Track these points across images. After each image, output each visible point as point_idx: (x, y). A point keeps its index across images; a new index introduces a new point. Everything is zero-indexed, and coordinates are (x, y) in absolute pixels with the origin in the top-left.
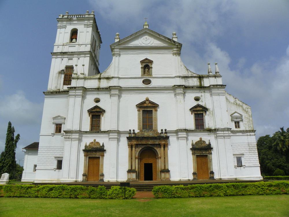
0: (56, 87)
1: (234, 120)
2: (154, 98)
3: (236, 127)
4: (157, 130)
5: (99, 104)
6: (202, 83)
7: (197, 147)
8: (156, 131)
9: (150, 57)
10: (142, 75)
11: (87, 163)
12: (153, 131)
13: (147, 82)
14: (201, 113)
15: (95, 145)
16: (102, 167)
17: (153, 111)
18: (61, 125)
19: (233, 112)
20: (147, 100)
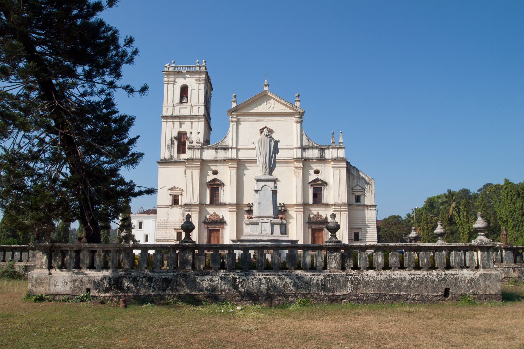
6: (324, 154)
14: (320, 186)
15: (214, 217)
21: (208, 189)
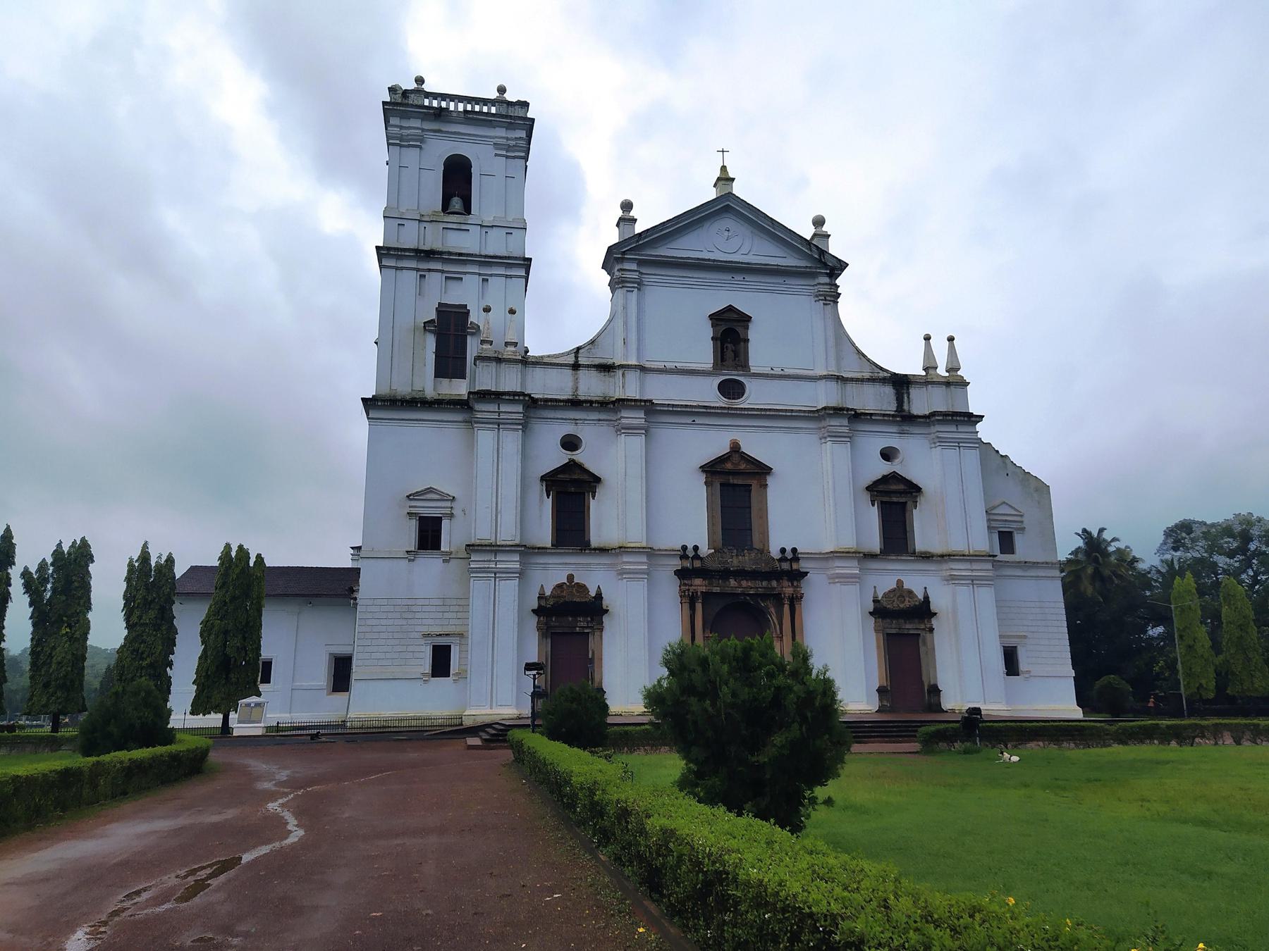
2: (758, 444)
5: (580, 456)
8: (764, 551)
10: (715, 364)
13: (731, 389)
14: (902, 500)
17: (753, 488)
18: (438, 521)
20: (735, 448)
21: (548, 498)
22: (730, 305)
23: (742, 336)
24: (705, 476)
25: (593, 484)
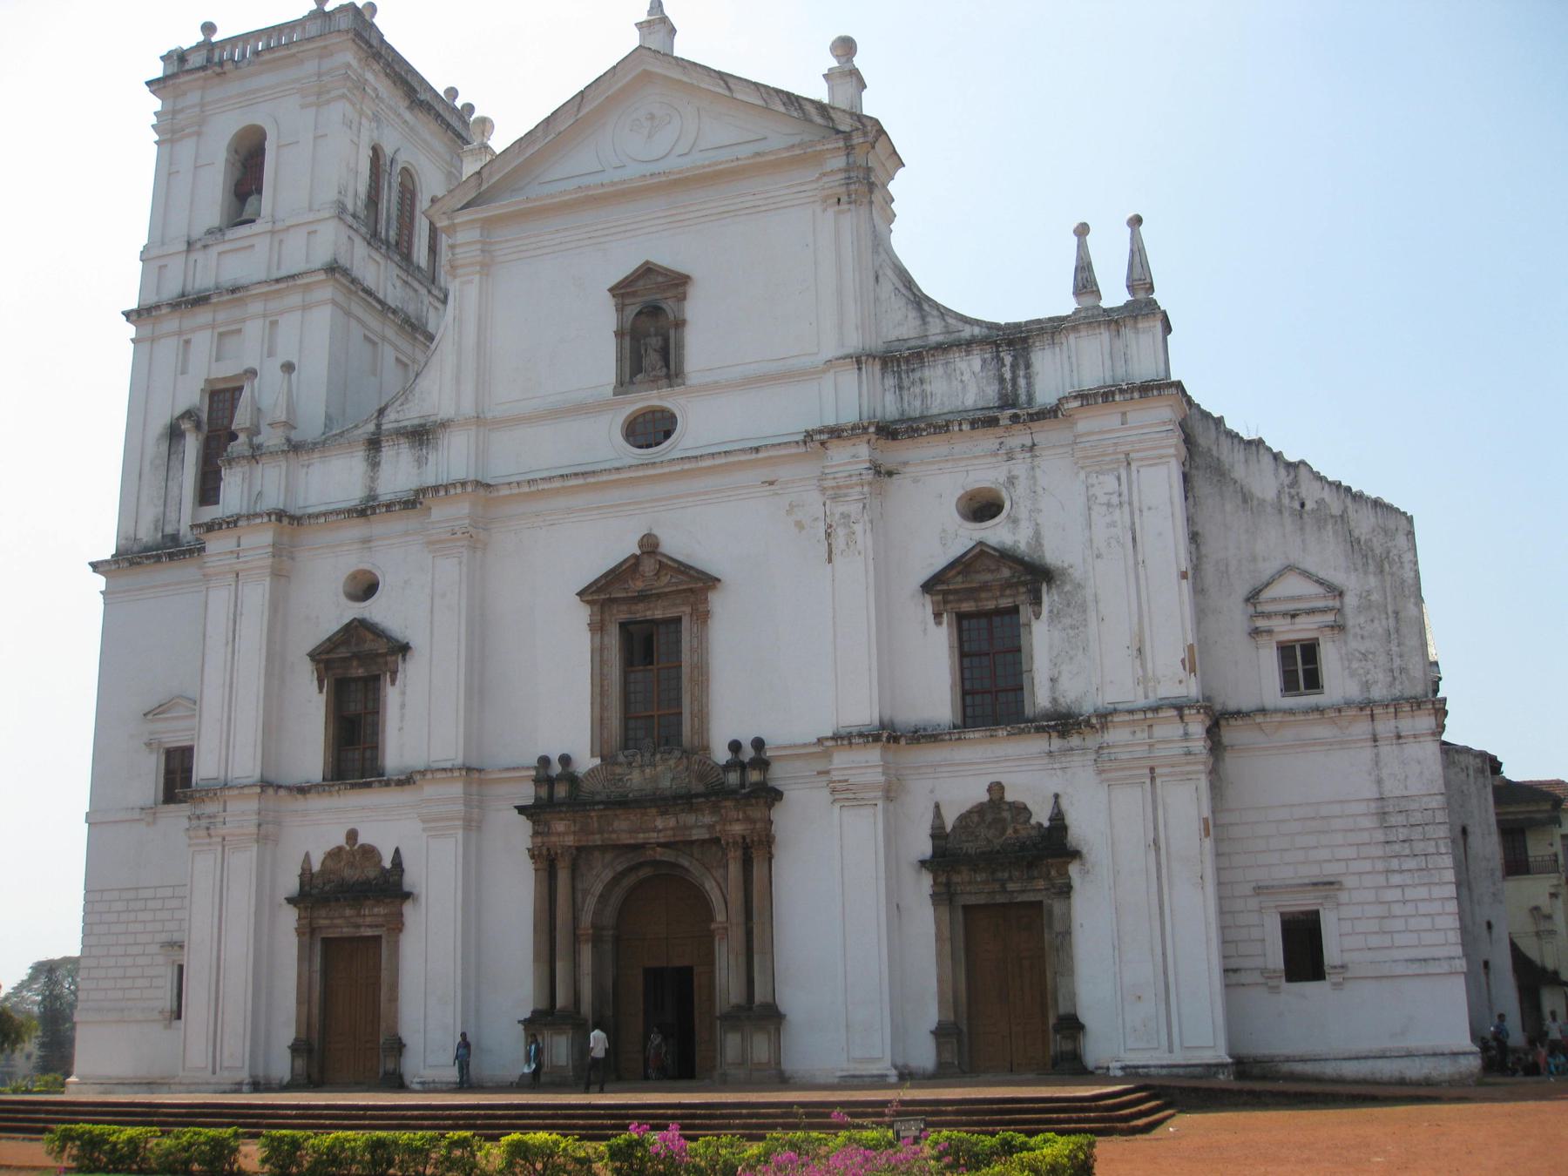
0: (160, 522)
1: (1270, 632)
3: (1290, 685)
4: (706, 748)
5: (376, 611)
6: (1022, 382)
7: (970, 847)
9: (666, 258)
11: (317, 977)
12: (677, 754)
14: (1005, 602)
16: (394, 998)
19: (1268, 569)
20: (649, 545)
21: (321, 691)
22: (647, 262)
23: (671, 317)
24: (589, 612)
25: (389, 658)
